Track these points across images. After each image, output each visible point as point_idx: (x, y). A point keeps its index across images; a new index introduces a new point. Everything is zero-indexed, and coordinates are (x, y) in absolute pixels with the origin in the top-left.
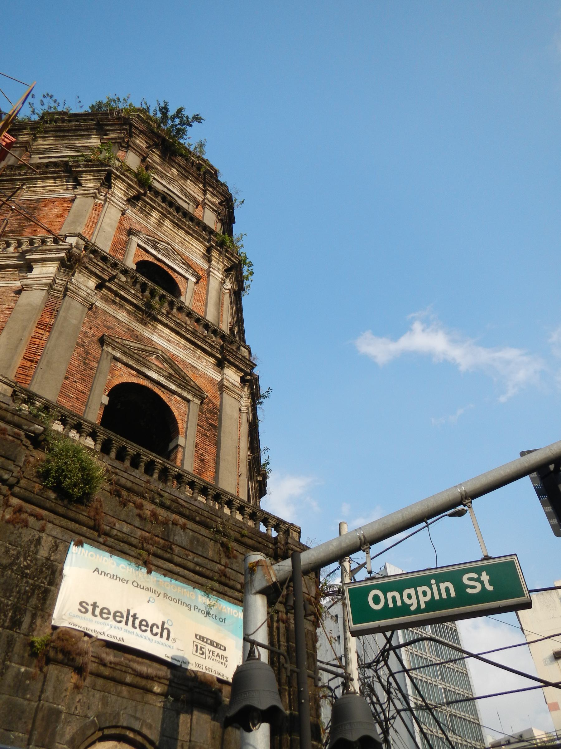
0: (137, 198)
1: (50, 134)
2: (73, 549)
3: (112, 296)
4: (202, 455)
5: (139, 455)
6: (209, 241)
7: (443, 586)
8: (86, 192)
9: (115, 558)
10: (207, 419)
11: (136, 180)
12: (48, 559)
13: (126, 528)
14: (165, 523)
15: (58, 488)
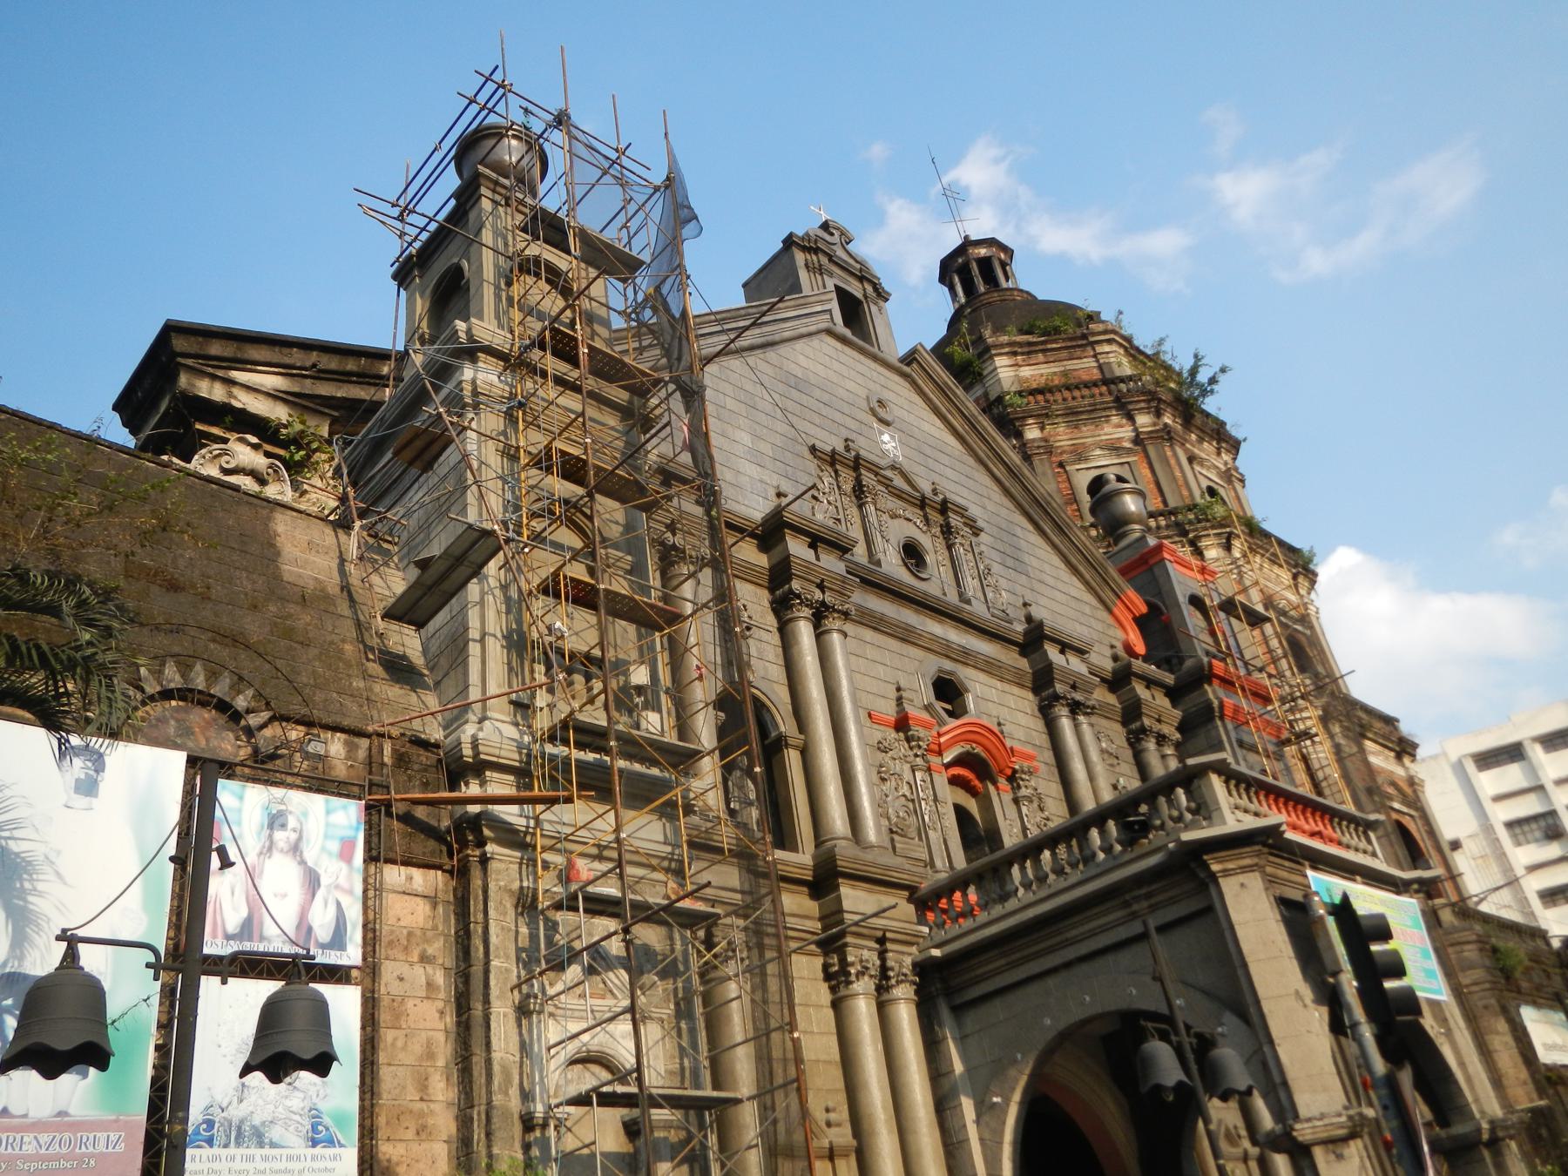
1: (1060, 420)
6: (1296, 566)
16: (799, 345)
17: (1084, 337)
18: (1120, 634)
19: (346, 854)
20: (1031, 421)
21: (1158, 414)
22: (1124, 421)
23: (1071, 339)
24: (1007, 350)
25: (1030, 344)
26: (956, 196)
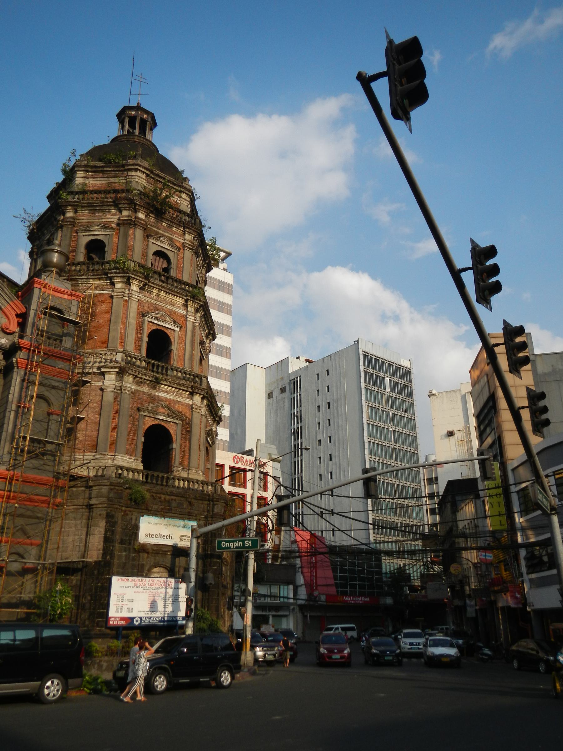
0: (145, 285)
1: (85, 208)
2: (141, 518)
3: (140, 380)
4: (183, 449)
5: (158, 476)
6: (186, 296)
7: (240, 543)
8: (118, 294)
9: (154, 517)
10: (185, 428)
11: (143, 276)
12: (135, 523)
13: (156, 507)
14: (169, 501)
15: (135, 501)
17: (123, 166)
20: (70, 208)
21: (135, 211)
22: (118, 213)
23: (117, 167)
24: (83, 169)
26: (142, 80)
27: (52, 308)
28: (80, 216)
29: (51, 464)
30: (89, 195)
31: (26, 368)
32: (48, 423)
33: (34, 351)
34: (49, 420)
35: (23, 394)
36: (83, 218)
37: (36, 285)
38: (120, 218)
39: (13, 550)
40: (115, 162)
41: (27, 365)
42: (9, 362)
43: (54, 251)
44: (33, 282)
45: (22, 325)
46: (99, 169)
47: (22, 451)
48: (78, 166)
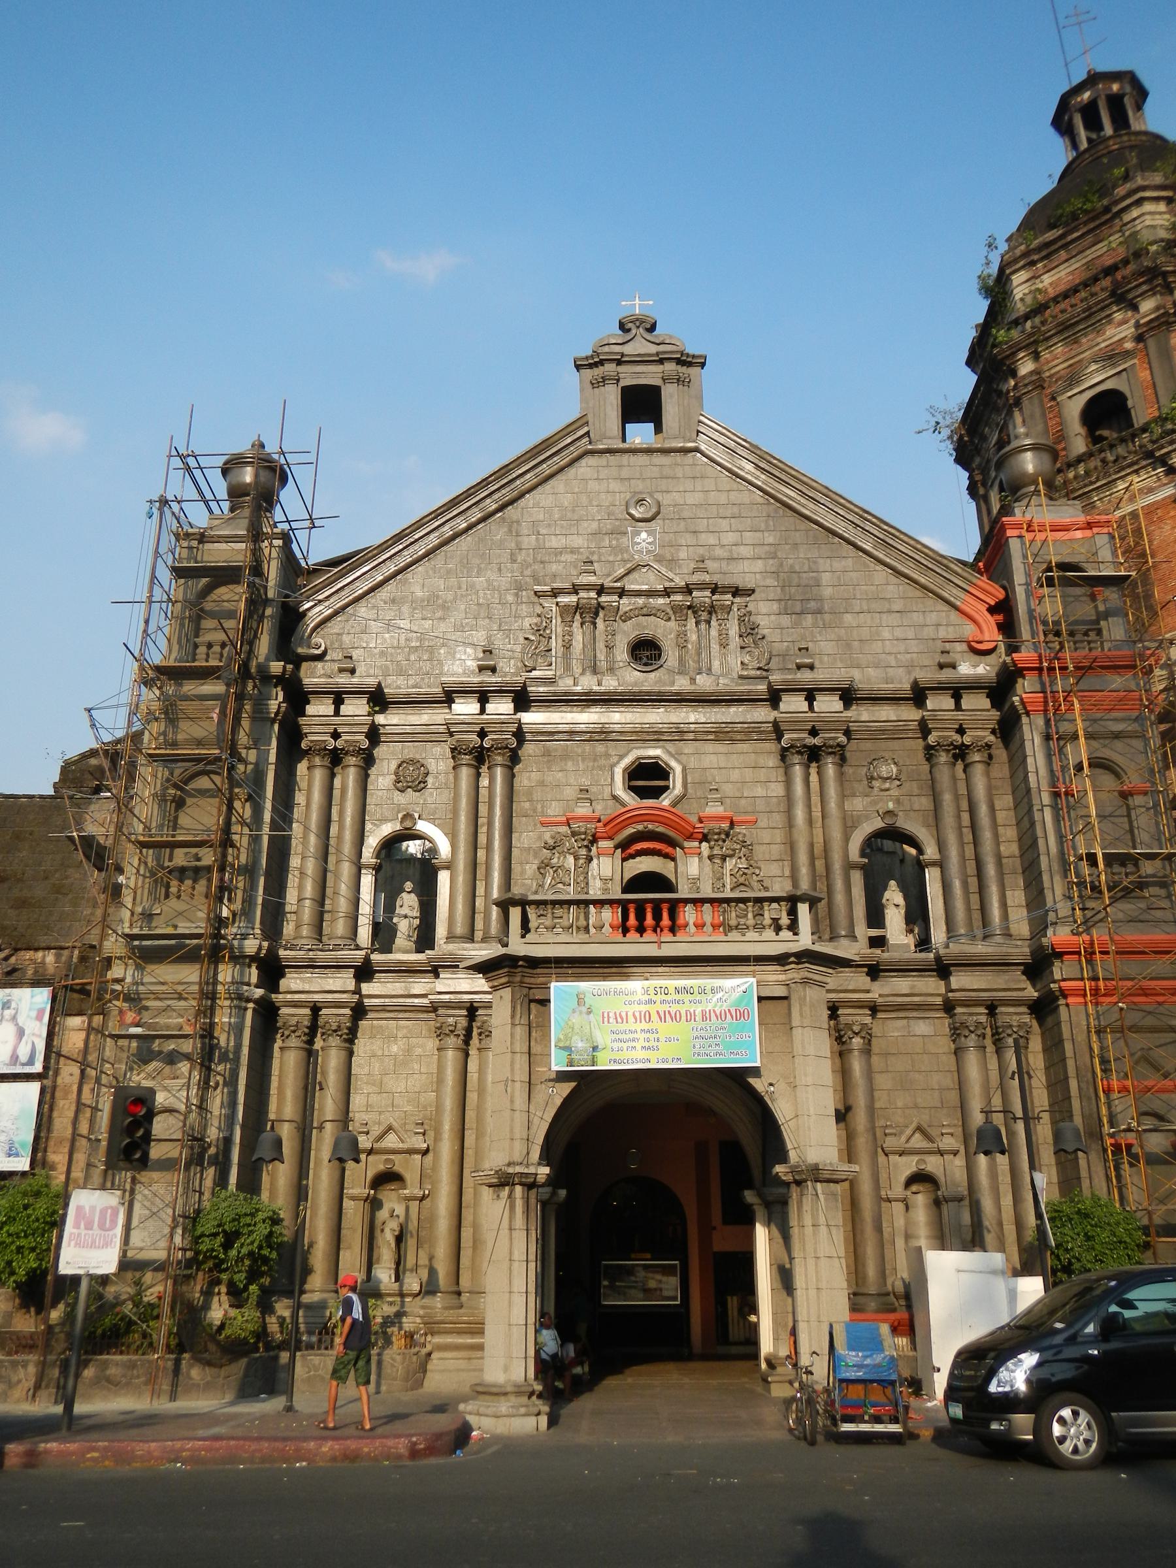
1: (1055, 340)
16: (548, 487)
18: (969, 630)
19: (39, 1018)
20: (1022, 355)
22: (1130, 313)
23: (1093, 219)
24: (1022, 263)
25: (1047, 245)
27: (1063, 567)
28: (1048, 362)
29: (1165, 904)
30: (1054, 310)
31: (1046, 711)
32: (1129, 816)
33: (1051, 669)
34: (1129, 809)
35: (1057, 766)
36: (1056, 362)
37: (1009, 533)
38: (1137, 322)
39: (1144, 1109)
40: (1086, 212)
41: (1046, 702)
42: (1006, 707)
43: (1022, 450)
44: (1003, 528)
45: (1008, 628)
46: (1056, 246)
47: (1096, 889)
48: (1009, 264)
